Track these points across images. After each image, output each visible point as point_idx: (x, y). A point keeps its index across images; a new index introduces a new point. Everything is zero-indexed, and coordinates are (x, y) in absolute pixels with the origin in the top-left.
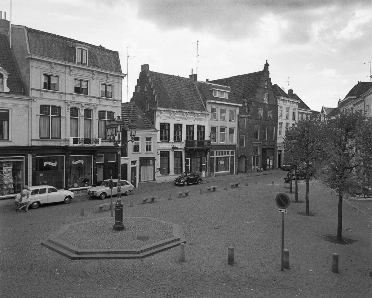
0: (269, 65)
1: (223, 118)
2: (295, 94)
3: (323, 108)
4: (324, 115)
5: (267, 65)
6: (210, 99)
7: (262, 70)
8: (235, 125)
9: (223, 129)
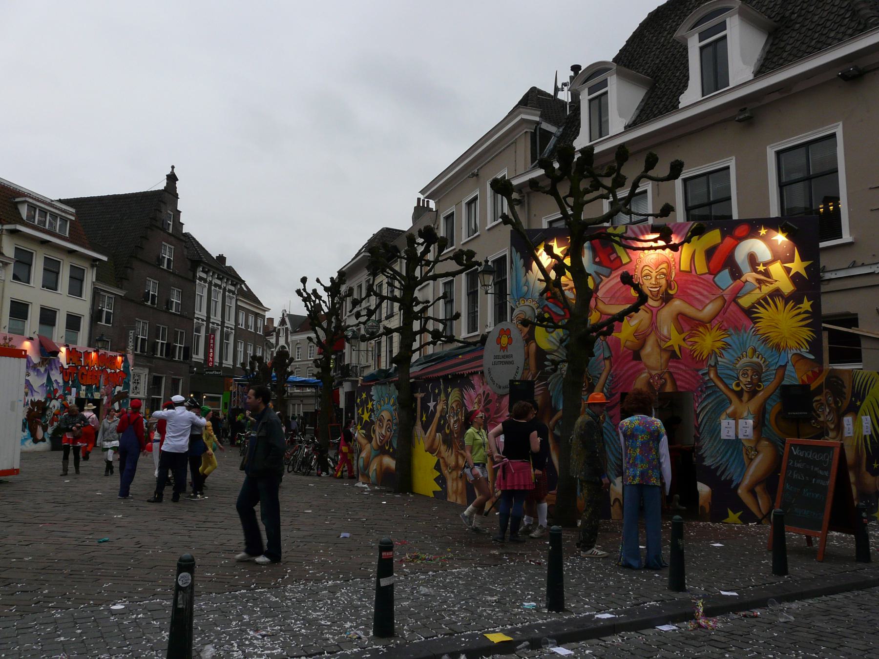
0: (177, 180)
1: (51, 284)
2: (230, 268)
3: (283, 314)
4: (287, 328)
5: (172, 178)
6: (16, 223)
7: (165, 185)
8: (82, 307)
9: (48, 317)
